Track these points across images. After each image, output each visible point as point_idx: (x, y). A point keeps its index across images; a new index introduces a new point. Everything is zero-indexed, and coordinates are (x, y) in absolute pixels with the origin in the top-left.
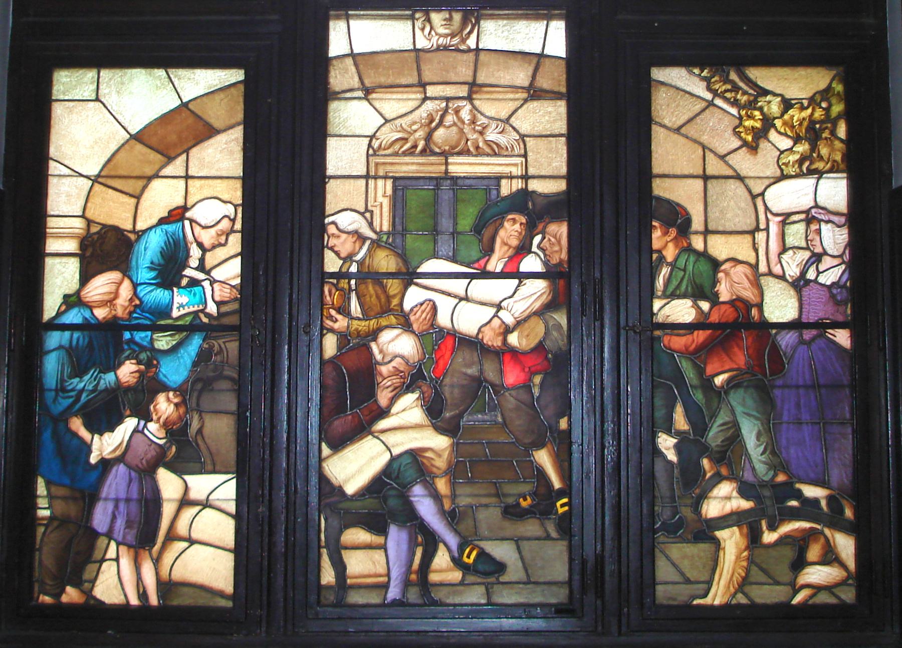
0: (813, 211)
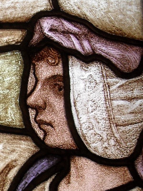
0: (47, 24)
